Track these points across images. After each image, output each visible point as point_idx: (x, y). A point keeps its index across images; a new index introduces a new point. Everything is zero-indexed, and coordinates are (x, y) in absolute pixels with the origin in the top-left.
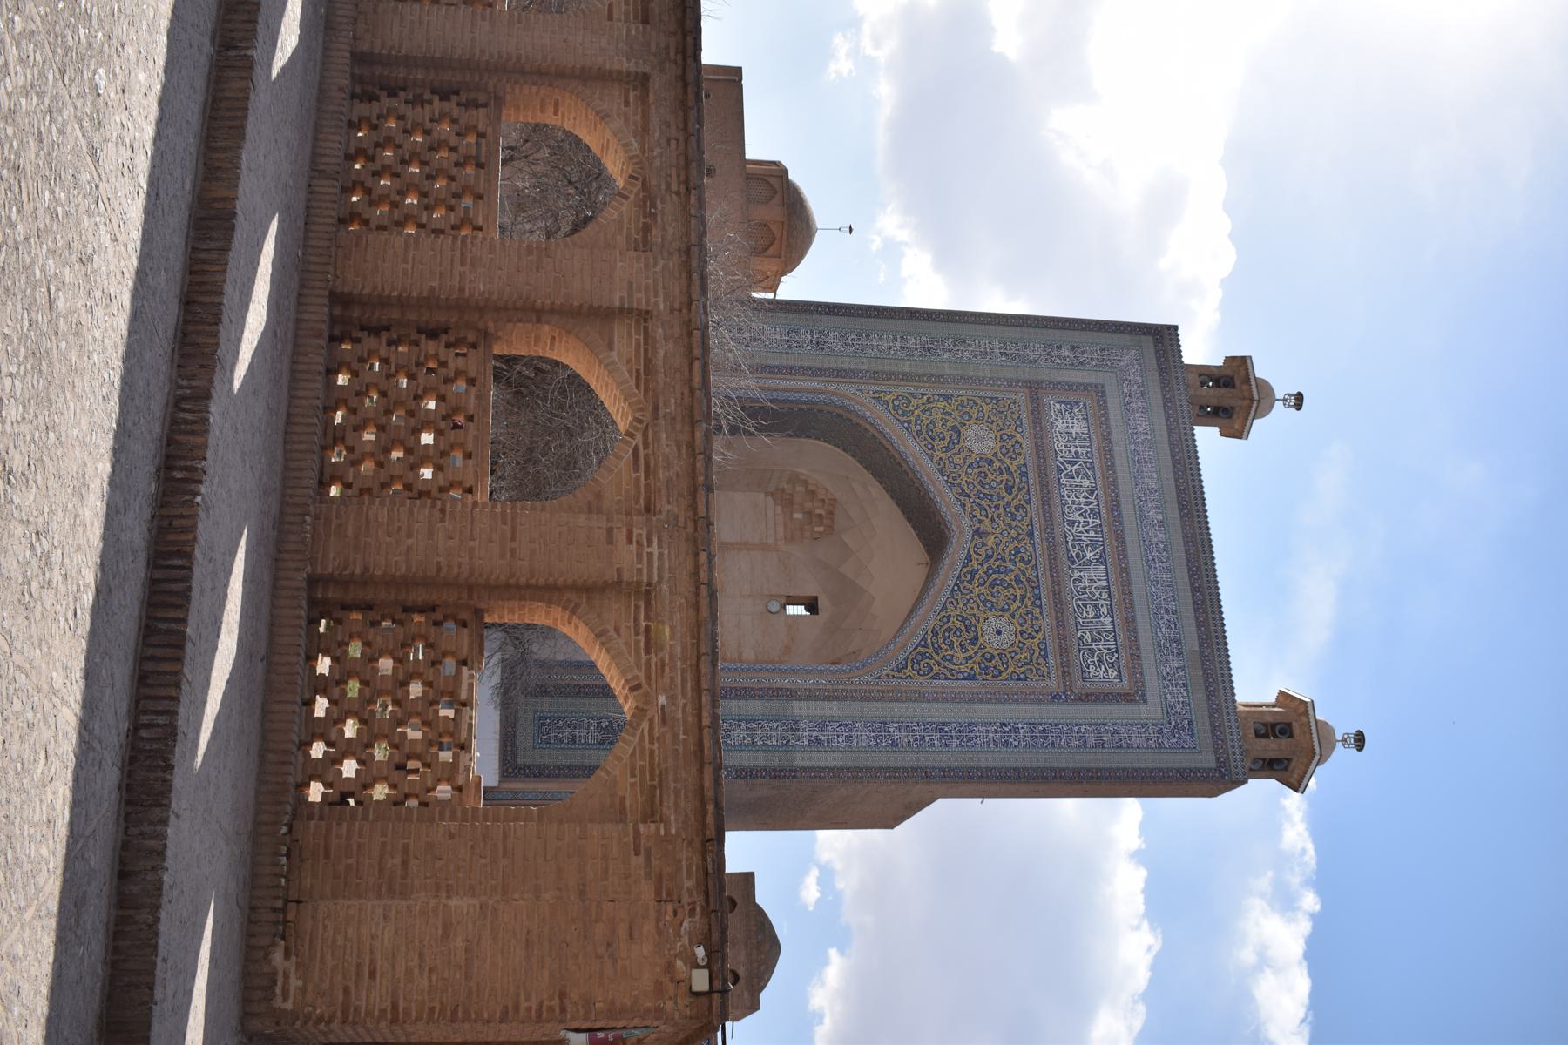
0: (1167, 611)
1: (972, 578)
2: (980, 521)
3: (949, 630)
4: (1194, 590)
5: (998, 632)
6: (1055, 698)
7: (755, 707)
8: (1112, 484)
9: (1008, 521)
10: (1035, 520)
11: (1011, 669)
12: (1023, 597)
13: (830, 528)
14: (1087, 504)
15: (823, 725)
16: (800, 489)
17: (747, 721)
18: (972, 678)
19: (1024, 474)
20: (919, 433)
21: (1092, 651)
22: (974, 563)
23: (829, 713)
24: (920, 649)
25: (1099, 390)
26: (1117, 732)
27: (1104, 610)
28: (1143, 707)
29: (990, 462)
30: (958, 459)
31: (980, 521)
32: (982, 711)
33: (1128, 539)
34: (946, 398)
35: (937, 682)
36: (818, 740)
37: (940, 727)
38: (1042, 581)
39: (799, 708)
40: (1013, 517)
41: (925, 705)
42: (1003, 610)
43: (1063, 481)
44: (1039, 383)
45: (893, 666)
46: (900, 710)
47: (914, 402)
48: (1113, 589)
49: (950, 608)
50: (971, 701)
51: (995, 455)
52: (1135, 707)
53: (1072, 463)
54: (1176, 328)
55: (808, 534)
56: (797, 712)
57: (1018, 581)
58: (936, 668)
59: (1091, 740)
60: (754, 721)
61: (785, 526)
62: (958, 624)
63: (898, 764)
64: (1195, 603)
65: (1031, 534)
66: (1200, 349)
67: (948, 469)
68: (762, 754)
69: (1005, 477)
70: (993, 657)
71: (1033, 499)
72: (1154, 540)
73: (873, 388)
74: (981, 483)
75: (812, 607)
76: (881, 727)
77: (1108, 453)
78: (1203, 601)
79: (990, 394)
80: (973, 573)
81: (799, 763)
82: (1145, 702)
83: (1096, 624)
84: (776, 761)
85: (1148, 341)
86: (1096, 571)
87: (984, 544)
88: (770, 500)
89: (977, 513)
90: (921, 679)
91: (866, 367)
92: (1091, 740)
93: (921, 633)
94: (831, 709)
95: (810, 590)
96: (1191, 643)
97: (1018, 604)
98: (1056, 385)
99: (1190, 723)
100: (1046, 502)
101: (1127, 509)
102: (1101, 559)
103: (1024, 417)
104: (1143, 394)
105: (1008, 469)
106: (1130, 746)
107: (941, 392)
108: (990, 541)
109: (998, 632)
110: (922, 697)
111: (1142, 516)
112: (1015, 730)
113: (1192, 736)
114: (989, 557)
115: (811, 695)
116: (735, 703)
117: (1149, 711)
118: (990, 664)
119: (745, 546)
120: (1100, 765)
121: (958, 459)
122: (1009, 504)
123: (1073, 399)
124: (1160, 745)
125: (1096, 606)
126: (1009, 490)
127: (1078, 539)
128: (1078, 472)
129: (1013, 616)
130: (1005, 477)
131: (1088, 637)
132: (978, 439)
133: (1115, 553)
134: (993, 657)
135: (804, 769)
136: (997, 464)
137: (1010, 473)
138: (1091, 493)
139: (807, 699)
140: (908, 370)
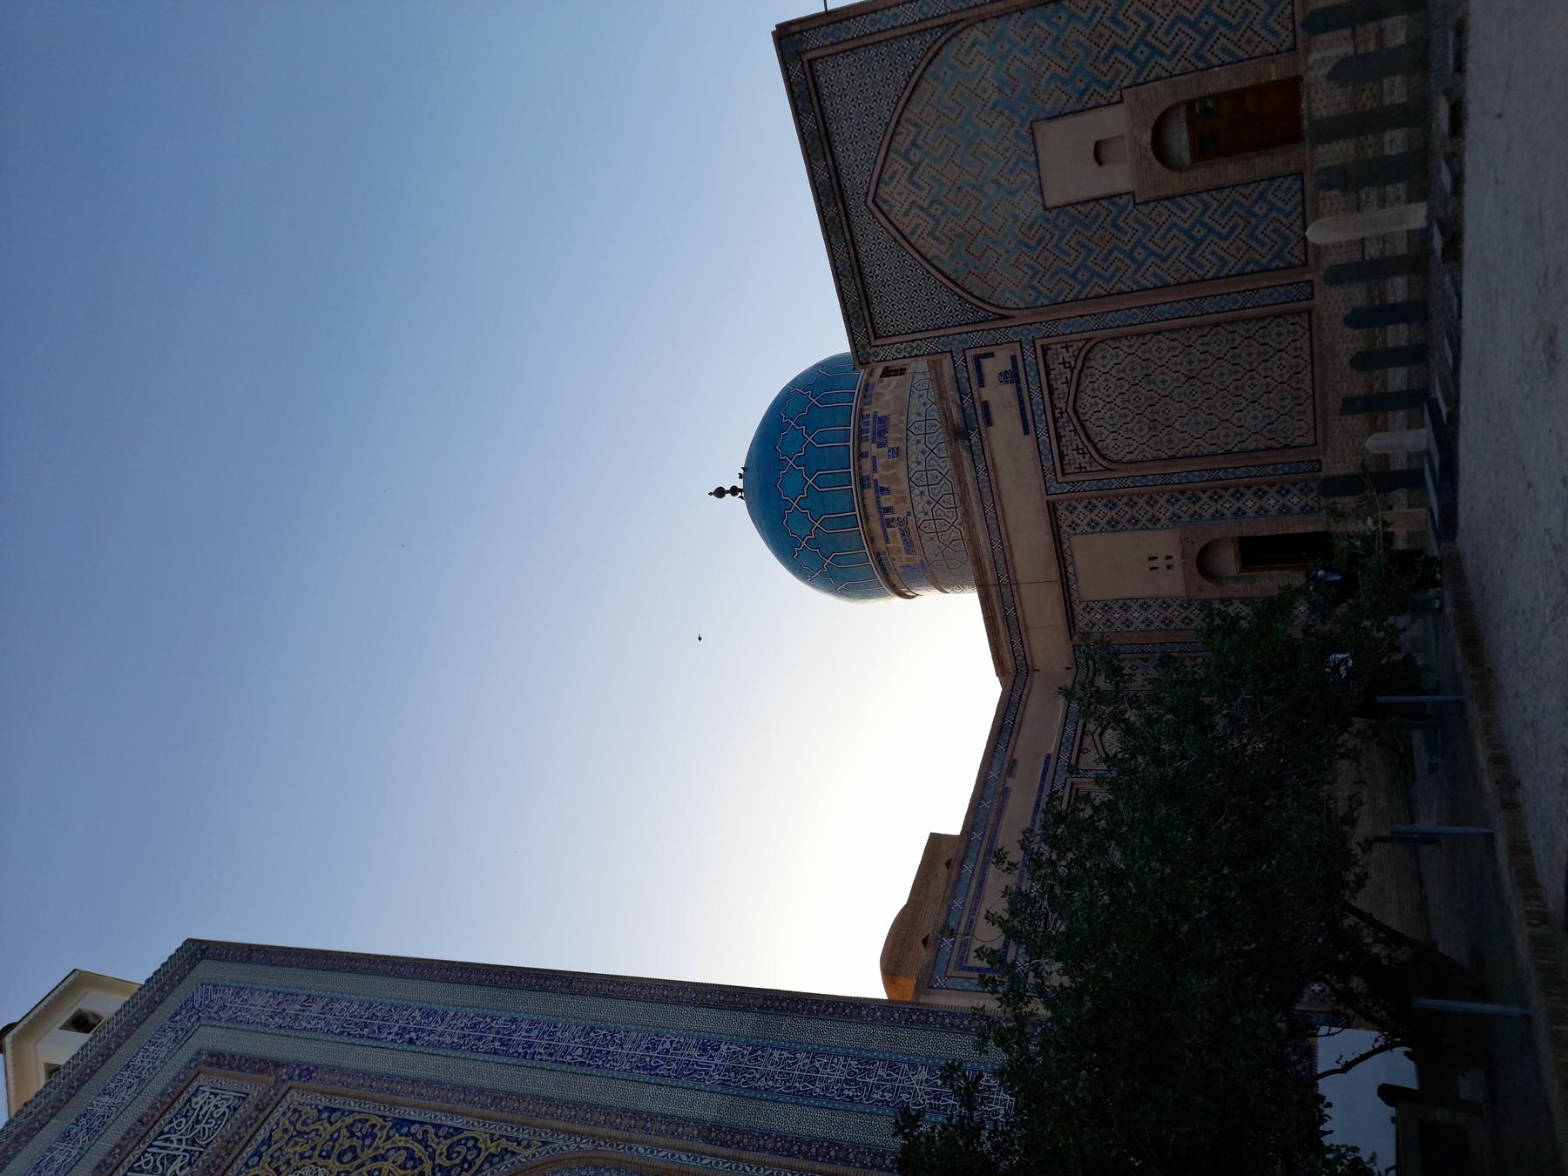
6: (307, 1072)
7: (788, 1119)
11: (330, 1129)
15: (686, 1071)
18: (400, 1123)
35: (458, 1123)
36: (703, 1049)
39: (705, 1106)
45: (508, 1159)
56: (716, 1099)
81: (750, 1018)
90: (480, 1132)
92: (315, 1008)
115: (674, 1124)
116: (818, 1131)
117: (209, 1038)
135: (747, 1009)
139: (686, 1121)
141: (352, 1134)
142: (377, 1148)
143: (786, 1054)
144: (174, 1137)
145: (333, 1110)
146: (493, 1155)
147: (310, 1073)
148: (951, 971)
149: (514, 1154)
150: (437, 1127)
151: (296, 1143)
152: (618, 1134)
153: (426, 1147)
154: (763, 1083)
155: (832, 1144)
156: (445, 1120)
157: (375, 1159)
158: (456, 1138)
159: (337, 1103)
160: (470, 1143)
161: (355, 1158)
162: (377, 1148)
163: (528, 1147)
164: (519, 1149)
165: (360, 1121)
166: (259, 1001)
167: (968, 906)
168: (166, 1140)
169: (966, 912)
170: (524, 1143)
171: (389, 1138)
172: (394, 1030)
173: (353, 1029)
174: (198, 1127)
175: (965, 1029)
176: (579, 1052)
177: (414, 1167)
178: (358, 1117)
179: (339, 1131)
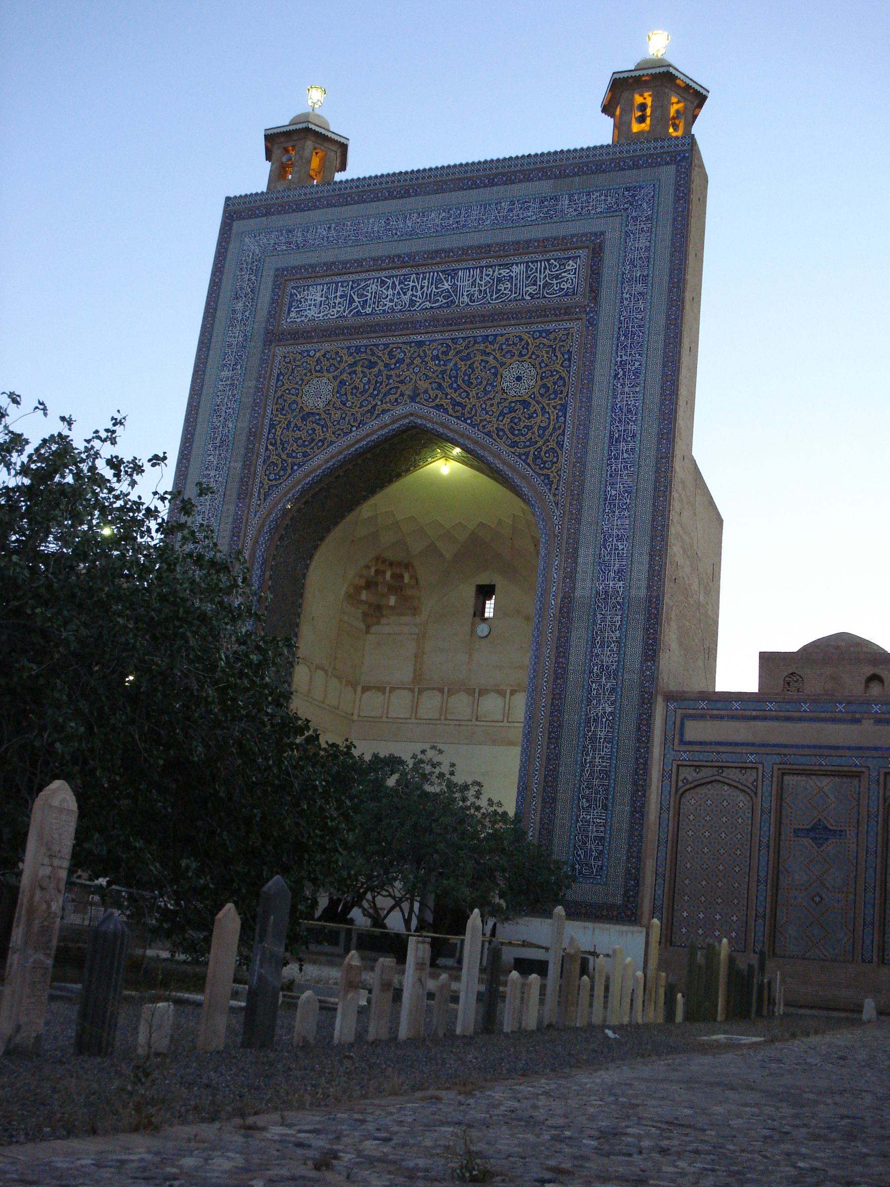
0: (511, 210)
1: (459, 404)
2: (402, 395)
3: (512, 430)
4: (492, 184)
5: (519, 379)
6: (592, 323)
8: (378, 264)
9: (404, 366)
10: (405, 339)
11: (558, 367)
13: (408, 566)
14: (394, 286)
15: (603, 566)
16: (364, 596)
17: (593, 645)
18: (564, 407)
19: (358, 349)
20: (305, 455)
21: (546, 285)
22: (444, 402)
23: (590, 559)
24: (530, 461)
25: (283, 276)
26: (632, 262)
27: (504, 272)
28: (608, 235)
29: (342, 383)
30: (337, 415)
31: (402, 395)
32: (600, 397)
33: (434, 247)
34: (272, 426)
35: (566, 443)
36: (619, 571)
37: (613, 441)
38: (469, 333)
39: (584, 589)
40: (401, 361)
41: (590, 457)
42: (495, 375)
43: (368, 310)
44: (267, 332)
46: (592, 483)
48: (484, 263)
49: (489, 428)
50: (589, 409)
52: (607, 243)
53: (352, 301)
54: (228, 199)
55: (410, 592)
57: (468, 357)
58: (552, 444)
59: (639, 287)
60: (594, 639)
61: (401, 614)
62: (507, 420)
63: (650, 487)
64: (505, 183)
65: (420, 344)
66: (254, 176)
67: (345, 426)
68: (630, 633)
69: (359, 369)
70: (544, 386)
71: (384, 340)
72: (437, 222)
73: (254, 500)
74: (365, 391)
75: (485, 592)
76: (609, 503)
77: (344, 268)
78: (503, 174)
79: (273, 382)
80: (455, 404)
82: (602, 233)
83: (518, 279)
84: (639, 618)
85: (237, 226)
86: (464, 280)
87: (426, 392)
88: (373, 629)
89: (393, 398)
90: (562, 460)
91: (232, 508)
92: (639, 287)
93: (511, 459)
94: (586, 556)
95: (469, 593)
96: (545, 187)
97: (492, 357)
98: (273, 315)
99: (628, 189)
100: (387, 328)
101: (403, 248)
102: (452, 274)
103: (300, 348)
104: (290, 231)
105: (351, 366)
106: (648, 249)
107: (266, 431)
108: (423, 385)
109: (519, 379)
110: (581, 461)
112: (622, 364)
113: (641, 188)
115: (571, 576)
116: (572, 659)
118: (552, 388)
119: (418, 656)
120: (666, 278)
122: (387, 365)
123: (287, 300)
124: (648, 219)
125: (499, 280)
126: (372, 365)
127: (429, 297)
128: (360, 296)
129: (502, 364)
130: (359, 369)
131: (531, 289)
133: (446, 260)
134: (544, 386)
135: (649, 588)
136: (344, 376)
138: (383, 283)
140: (239, 465)
141: (555, 383)
142: (548, 405)
143: (618, 624)
144: (547, 271)
145: (569, 360)
146: (548, 479)
147: (591, 324)
148: (679, 711)
149: (550, 490)
150: (563, 435)
151: (547, 352)
152: (564, 545)
153: (551, 435)
154: (599, 616)
155: (565, 670)
156: (567, 433)
157: (543, 408)
158: (557, 449)
159: (575, 357)
160: (555, 460)
161: (542, 395)
162: (548, 405)
163: (555, 495)
164: (553, 490)
165: (565, 382)
167: (736, 713)
168: (545, 268)
169: (729, 712)
170: (557, 492)
171: (554, 407)
172: (624, 358)
173: (624, 325)
174: (555, 282)
175: (639, 728)
176: (614, 493)
177: (539, 436)
178: (566, 379)
179: (558, 372)
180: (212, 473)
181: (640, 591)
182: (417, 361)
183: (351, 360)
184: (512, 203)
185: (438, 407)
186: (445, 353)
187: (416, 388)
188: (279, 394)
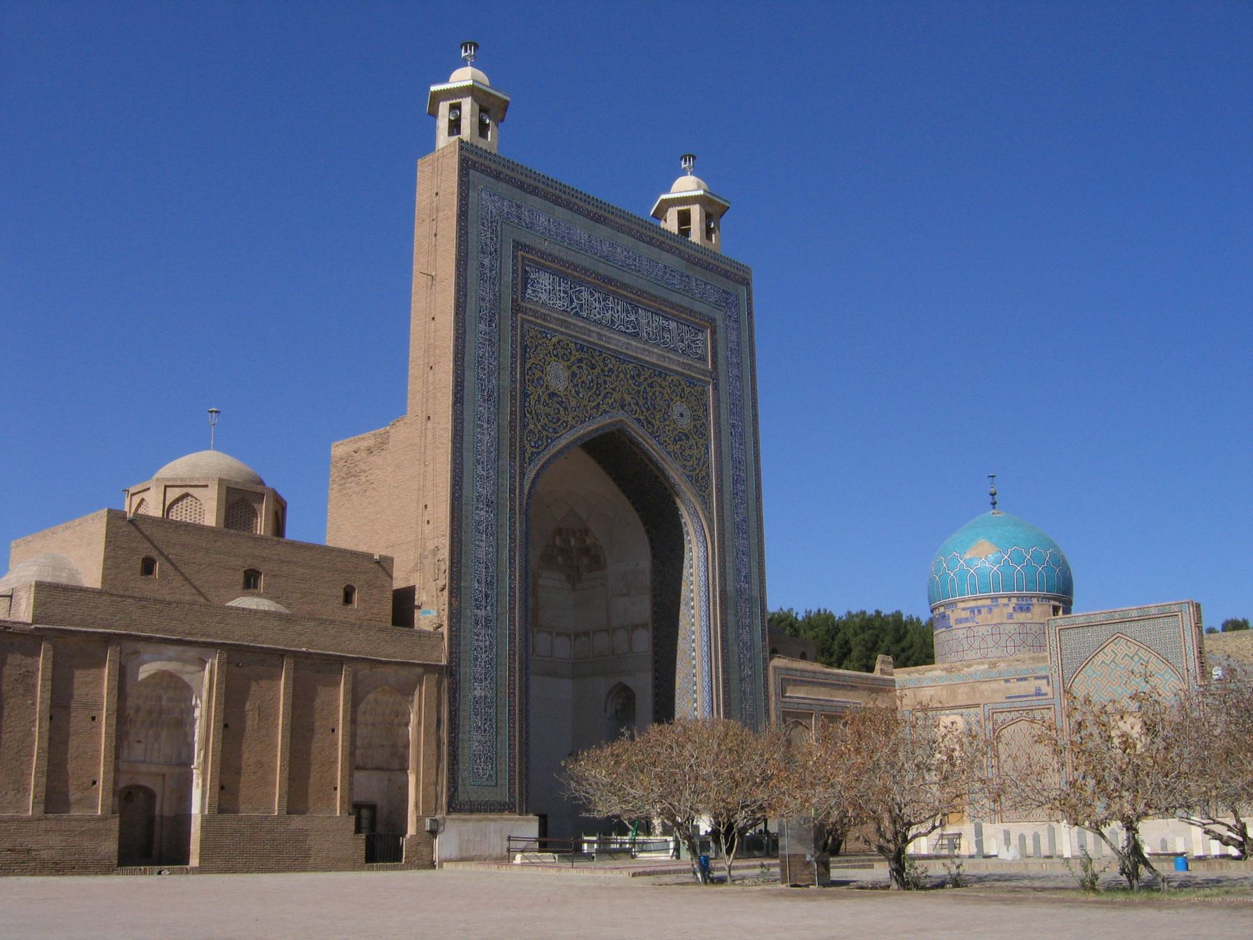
9: (614, 376)
12: (660, 386)
18: (707, 448)
20: (555, 431)
30: (574, 403)
37: (735, 482)
39: (730, 588)
40: (611, 370)
42: (669, 406)
47: (531, 426)
51: (569, 367)
58: (704, 473)
74: (590, 388)
80: (649, 422)
92: (736, 371)
108: (628, 398)
111: (607, 258)
114: (637, 404)
121: (574, 403)
122: (603, 371)
126: (593, 367)
128: (578, 299)
132: (557, 377)
137: (580, 360)
166: (734, 338)
180: (485, 426)
181: (756, 593)
182: (622, 376)
183: (578, 357)
184: (665, 267)
185: (638, 420)
186: (638, 375)
187: (622, 399)
188: (528, 366)
